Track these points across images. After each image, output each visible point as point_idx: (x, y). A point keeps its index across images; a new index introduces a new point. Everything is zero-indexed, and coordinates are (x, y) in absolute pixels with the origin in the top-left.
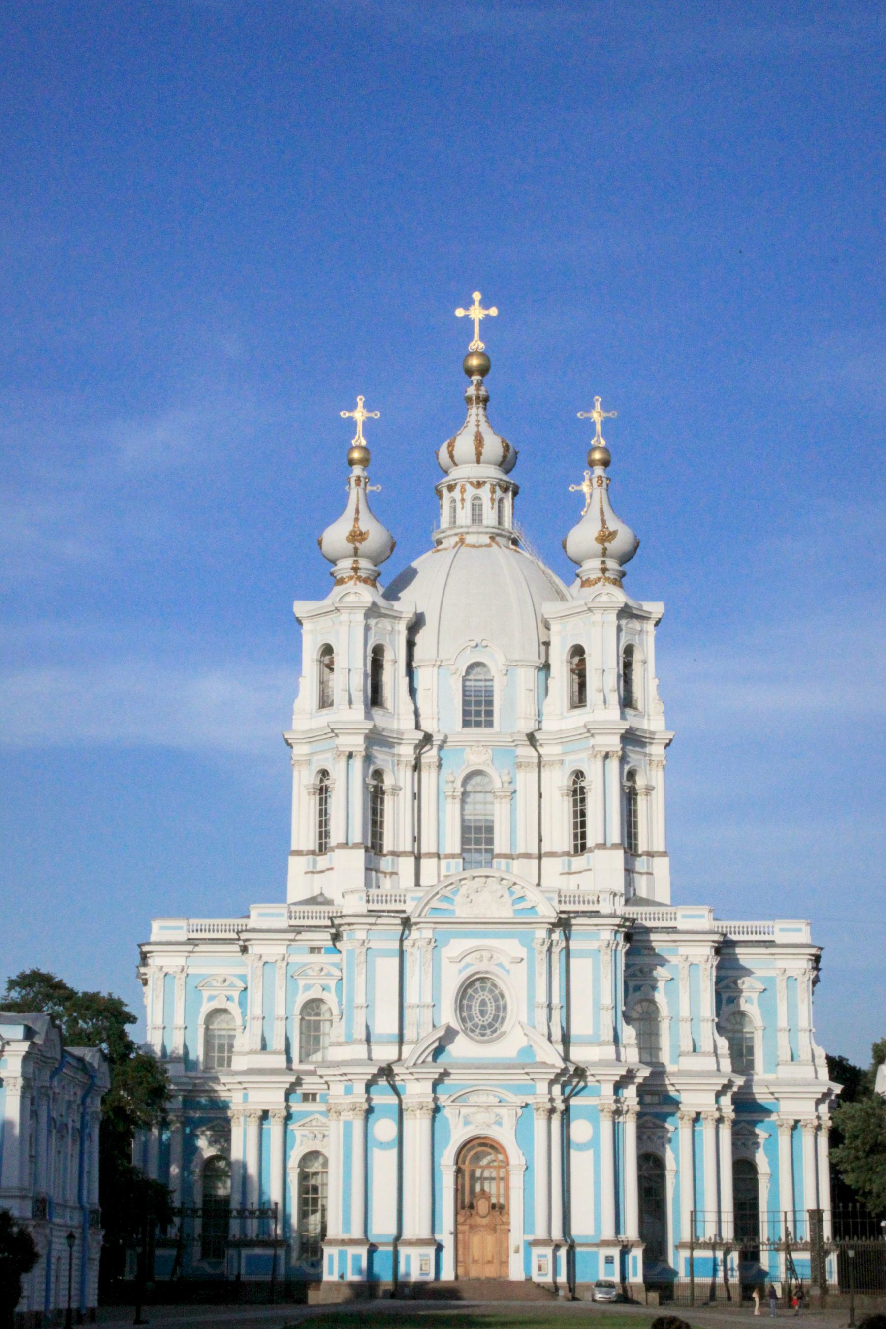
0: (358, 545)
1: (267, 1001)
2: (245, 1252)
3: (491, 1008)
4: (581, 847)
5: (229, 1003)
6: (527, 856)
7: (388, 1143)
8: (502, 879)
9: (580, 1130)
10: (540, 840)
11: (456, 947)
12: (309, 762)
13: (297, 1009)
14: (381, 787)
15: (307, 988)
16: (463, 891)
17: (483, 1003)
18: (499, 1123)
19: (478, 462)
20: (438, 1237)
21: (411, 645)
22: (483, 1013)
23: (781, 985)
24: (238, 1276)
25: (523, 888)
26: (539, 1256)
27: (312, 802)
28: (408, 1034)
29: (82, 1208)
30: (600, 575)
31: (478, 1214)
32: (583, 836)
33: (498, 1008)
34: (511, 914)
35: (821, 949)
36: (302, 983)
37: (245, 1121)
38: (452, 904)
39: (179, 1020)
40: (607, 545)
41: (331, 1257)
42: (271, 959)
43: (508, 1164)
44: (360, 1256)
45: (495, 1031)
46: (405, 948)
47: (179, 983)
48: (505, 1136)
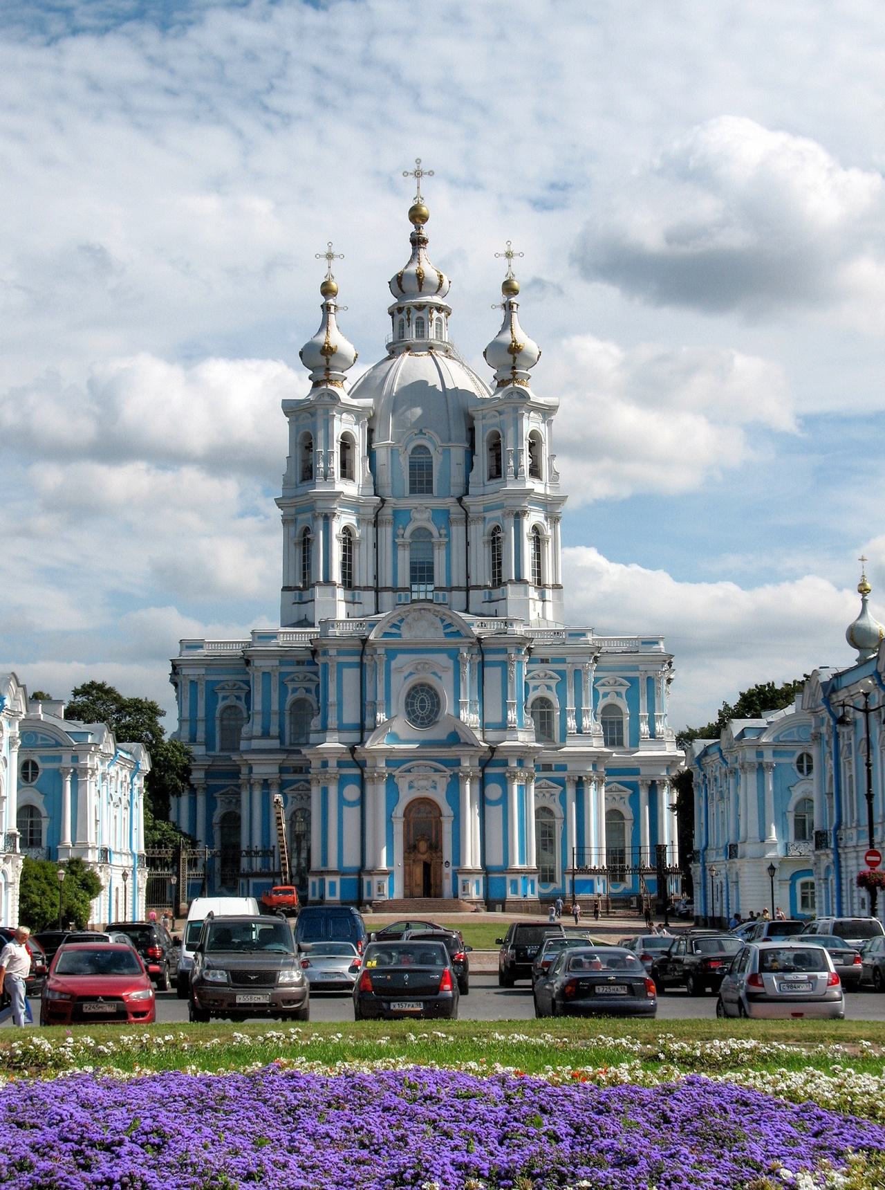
0: (329, 357)
2: (252, 881)
3: (428, 705)
4: (498, 582)
5: (238, 702)
6: (458, 589)
7: (354, 802)
8: (435, 611)
9: (493, 791)
10: (468, 577)
11: (401, 659)
12: (295, 521)
13: (287, 707)
14: (349, 539)
15: (295, 690)
17: (422, 701)
18: (435, 788)
19: (420, 290)
20: (391, 868)
21: (371, 431)
23: (643, 685)
25: (450, 617)
26: (463, 881)
27: (298, 550)
28: (368, 722)
29: (133, 854)
30: (511, 377)
32: (500, 575)
33: (433, 704)
34: (443, 635)
35: (672, 656)
36: (290, 686)
38: (399, 629)
39: (201, 713)
40: (516, 355)
41: (314, 884)
42: (267, 670)
43: (441, 815)
45: (431, 720)
46: (365, 661)
47: (201, 688)
48: (439, 796)
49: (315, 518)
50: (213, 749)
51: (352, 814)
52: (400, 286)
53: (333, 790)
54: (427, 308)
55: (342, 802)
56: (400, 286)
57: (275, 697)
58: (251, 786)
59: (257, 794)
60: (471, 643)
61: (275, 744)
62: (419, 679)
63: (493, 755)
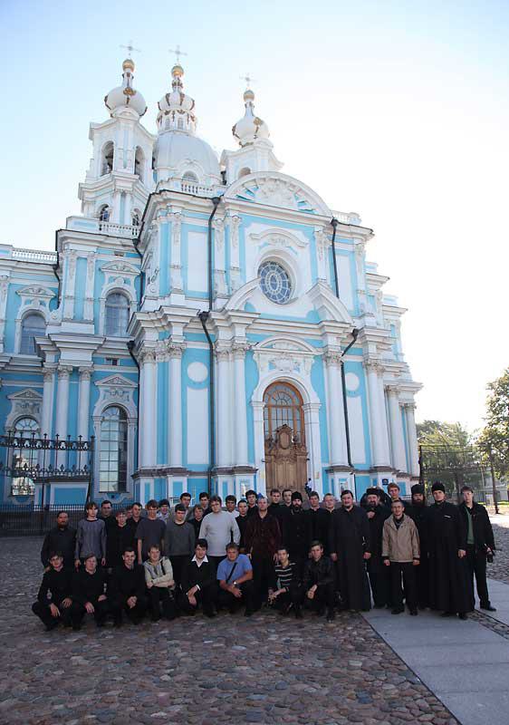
1: (79, 284)
2: (54, 486)
7: (200, 383)
8: (291, 185)
11: (257, 228)
13: (103, 295)
16: (261, 188)
17: (273, 279)
18: (298, 370)
22: (274, 286)
24: (48, 506)
25: (306, 194)
31: (281, 446)
37: (56, 379)
41: (147, 486)
44: (181, 483)
46: (213, 226)
48: (303, 378)
49: (113, 196)
50: (12, 352)
51: (199, 399)
52: (168, 100)
53: (176, 363)
54: (186, 114)
55: (186, 383)
56: (168, 100)
57: (90, 284)
58: (58, 372)
59: (64, 383)
60: (326, 222)
61: (89, 329)
62: (273, 251)
63: (353, 343)
